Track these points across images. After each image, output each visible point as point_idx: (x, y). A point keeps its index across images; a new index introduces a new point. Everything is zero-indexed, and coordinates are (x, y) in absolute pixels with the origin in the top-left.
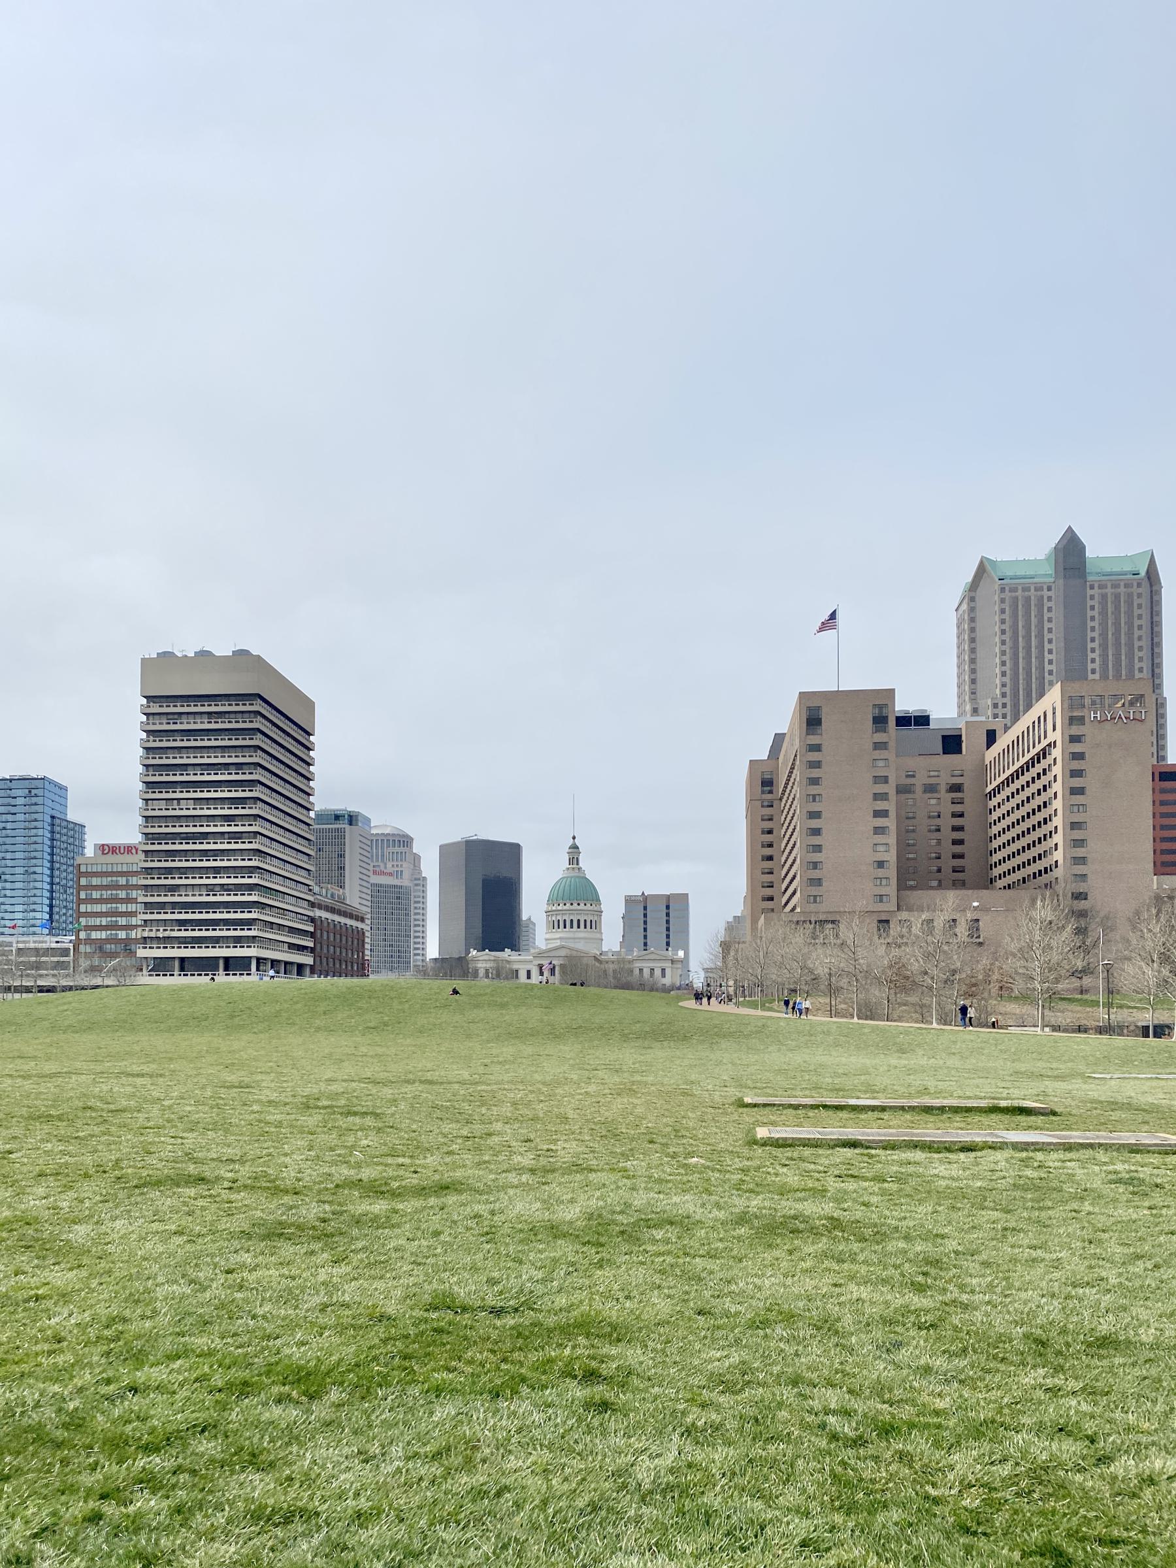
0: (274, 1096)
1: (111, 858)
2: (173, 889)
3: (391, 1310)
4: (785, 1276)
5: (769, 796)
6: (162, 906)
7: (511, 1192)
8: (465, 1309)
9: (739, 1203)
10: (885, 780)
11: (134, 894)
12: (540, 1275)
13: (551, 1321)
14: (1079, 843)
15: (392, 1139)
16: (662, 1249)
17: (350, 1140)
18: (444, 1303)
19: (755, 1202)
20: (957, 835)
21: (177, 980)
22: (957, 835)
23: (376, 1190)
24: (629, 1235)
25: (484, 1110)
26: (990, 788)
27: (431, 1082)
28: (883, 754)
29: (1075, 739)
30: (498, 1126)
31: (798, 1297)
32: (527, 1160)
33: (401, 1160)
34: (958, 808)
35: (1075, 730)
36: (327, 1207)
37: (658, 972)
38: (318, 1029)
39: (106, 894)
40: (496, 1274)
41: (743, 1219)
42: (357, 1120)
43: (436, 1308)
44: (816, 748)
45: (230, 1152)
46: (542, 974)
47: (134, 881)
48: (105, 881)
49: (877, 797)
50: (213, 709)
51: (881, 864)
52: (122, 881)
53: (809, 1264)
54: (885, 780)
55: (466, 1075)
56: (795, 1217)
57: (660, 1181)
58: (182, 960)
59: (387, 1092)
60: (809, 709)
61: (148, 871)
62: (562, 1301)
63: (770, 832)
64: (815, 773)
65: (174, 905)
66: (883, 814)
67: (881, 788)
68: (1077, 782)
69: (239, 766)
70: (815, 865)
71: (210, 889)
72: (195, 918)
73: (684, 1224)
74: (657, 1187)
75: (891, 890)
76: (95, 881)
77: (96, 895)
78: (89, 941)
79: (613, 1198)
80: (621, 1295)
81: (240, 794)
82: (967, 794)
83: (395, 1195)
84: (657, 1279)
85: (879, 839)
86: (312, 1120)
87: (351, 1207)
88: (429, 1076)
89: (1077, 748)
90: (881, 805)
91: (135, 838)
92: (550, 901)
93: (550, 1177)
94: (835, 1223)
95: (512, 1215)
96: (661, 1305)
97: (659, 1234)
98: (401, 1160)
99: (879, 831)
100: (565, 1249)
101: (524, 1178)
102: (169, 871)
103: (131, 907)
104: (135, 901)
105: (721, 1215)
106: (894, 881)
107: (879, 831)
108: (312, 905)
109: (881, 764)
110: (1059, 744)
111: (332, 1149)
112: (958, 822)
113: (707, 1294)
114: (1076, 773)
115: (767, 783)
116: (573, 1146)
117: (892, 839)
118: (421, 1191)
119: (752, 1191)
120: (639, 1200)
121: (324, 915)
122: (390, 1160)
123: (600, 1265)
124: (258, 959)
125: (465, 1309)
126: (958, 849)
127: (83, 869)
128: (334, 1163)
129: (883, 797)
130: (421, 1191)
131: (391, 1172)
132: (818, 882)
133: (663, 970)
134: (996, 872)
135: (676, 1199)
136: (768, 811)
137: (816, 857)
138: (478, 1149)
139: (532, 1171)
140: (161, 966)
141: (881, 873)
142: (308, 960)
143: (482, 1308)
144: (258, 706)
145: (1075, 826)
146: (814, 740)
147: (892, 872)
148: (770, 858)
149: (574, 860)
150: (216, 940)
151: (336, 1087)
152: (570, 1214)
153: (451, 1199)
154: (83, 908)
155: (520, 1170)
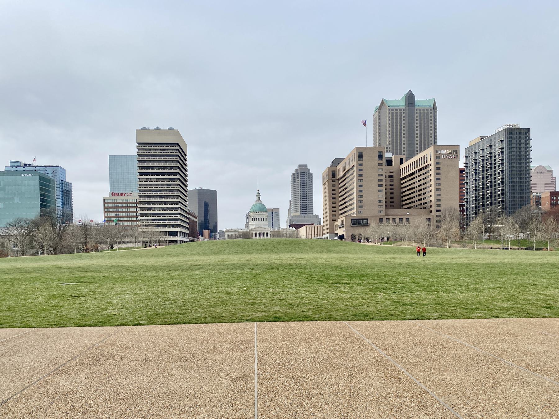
1: (116, 197)
2: (150, 209)
10: (382, 175)
14: (438, 195)
20: (391, 191)
22: (391, 191)
26: (402, 177)
28: (381, 167)
29: (437, 163)
34: (391, 183)
35: (438, 161)
44: (361, 165)
48: (114, 205)
51: (380, 201)
52: (120, 205)
54: (382, 175)
60: (359, 152)
64: (361, 173)
65: (151, 214)
66: (381, 186)
67: (380, 178)
68: (438, 176)
69: (172, 167)
70: (361, 202)
71: (163, 209)
75: (383, 209)
76: (110, 205)
77: (111, 210)
82: (395, 178)
85: (380, 193)
89: (438, 166)
90: (380, 183)
99: (380, 191)
102: (148, 202)
106: (384, 206)
107: (380, 191)
110: (432, 164)
112: (392, 187)
114: (438, 174)
117: (384, 193)
126: (392, 196)
129: (381, 180)
132: (361, 207)
134: (404, 203)
137: (361, 199)
141: (380, 204)
145: (437, 190)
146: (360, 162)
147: (383, 204)
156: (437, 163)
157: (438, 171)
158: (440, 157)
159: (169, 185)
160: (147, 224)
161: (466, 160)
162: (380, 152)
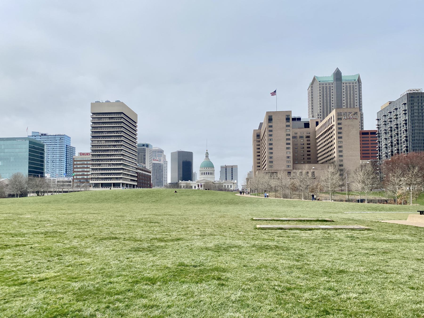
0: (130, 219)
1: (83, 156)
2: (99, 165)
3: (169, 266)
4: (265, 258)
5: (259, 139)
6: (96, 169)
7: (195, 240)
8: (187, 266)
9: (253, 242)
10: (289, 135)
11: (89, 166)
12: (205, 258)
13: (208, 268)
15: (163, 228)
16: (234, 252)
17: (152, 229)
18: (182, 264)
19: (257, 242)
21: (100, 189)
23: (161, 240)
24: (226, 250)
25: (186, 222)
27: (171, 215)
28: (289, 128)
30: (190, 225)
31: (268, 263)
32: (199, 233)
33: (166, 233)
34: (309, 142)
36: (149, 244)
37: (229, 186)
38: (139, 202)
39: (81, 166)
40: (194, 258)
41: (254, 246)
42: (153, 224)
43: (180, 266)
44: (271, 126)
45: (122, 232)
46: (198, 187)
47: (89, 162)
48: (81, 163)
49: (288, 139)
50: (110, 116)
51: (288, 157)
52: (86, 162)
53: (270, 256)
54: (289, 135)
55: (180, 213)
56: (267, 246)
57: (233, 238)
58: (102, 184)
59: (160, 217)
60: (269, 116)
61: (93, 160)
62: (211, 264)
63: (259, 149)
64: (271, 133)
65: (100, 169)
67: (288, 137)
68: (340, 135)
69: (117, 132)
70: (271, 158)
71: (109, 164)
72: (106, 173)
73: (239, 247)
74: (232, 239)
75: (291, 164)
76: (78, 163)
77: (78, 166)
78: (77, 179)
79: (221, 242)
80: (225, 263)
81: (117, 139)
82: (311, 139)
83: (165, 241)
84: (233, 259)
85: (288, 150)
86: (142, 224)
87: (155, 244)
88: (170, 213)
90: (288, 142)
91: (89, 151)
92: (201, 167)
93: (205, 237)
94: (277, 247)
95: (196, 245)
96: (235, 265)
97: (233, 249)
98: (166, 233)
99: (288, 148)
100: (210, 253)
101: (198, 237)
103: (88, 170)
104: (89, 168)
105: (249, 245)
106: (292, 162)
107: (288, 148)
108: (137, 169)
109: (288, 131)
111: (148, 231)
112: (309, 146)
113: (246, 262)
115: (258, 136)
116: (210, 230)
117: (291, 150)
118: (172, 240)
119: (256, 240)
120: (228, 242)
121: (140, 171)
122: (163, 233)
123: (219, 256)
124: (122, 183)
125: (187, 266)
126: (309, 153)
127: (75, 159)
128: (149, 234)
130: (172, 240)
131: (164, 236)
132: (271, 162)
133: (231, 186)
134: (319, 159)
135: (237, 242)
136: (258, 143)
137: (271, 155)
138: (186, 231)
139: (200, 236)
140: (96, 185)
141: (288, 159)
142: (136, 184)
143: (191, 266)
144: (122, 116)
145: (340, 147)
146: (270, 124)
147: (291, 159)
148: (259, 156)
149: (207, 156)
150: (111, 179)
151: (147, 216)
152: (210, 245)
153: (180, 242)
154: (75, 170)
155: (197, 235)
156: (339, 124)
157: (340, 131)
158: (341, 118)
159: (115, 146)
160: (96, 177)
161: (378, 122)
162: (288, 116)
